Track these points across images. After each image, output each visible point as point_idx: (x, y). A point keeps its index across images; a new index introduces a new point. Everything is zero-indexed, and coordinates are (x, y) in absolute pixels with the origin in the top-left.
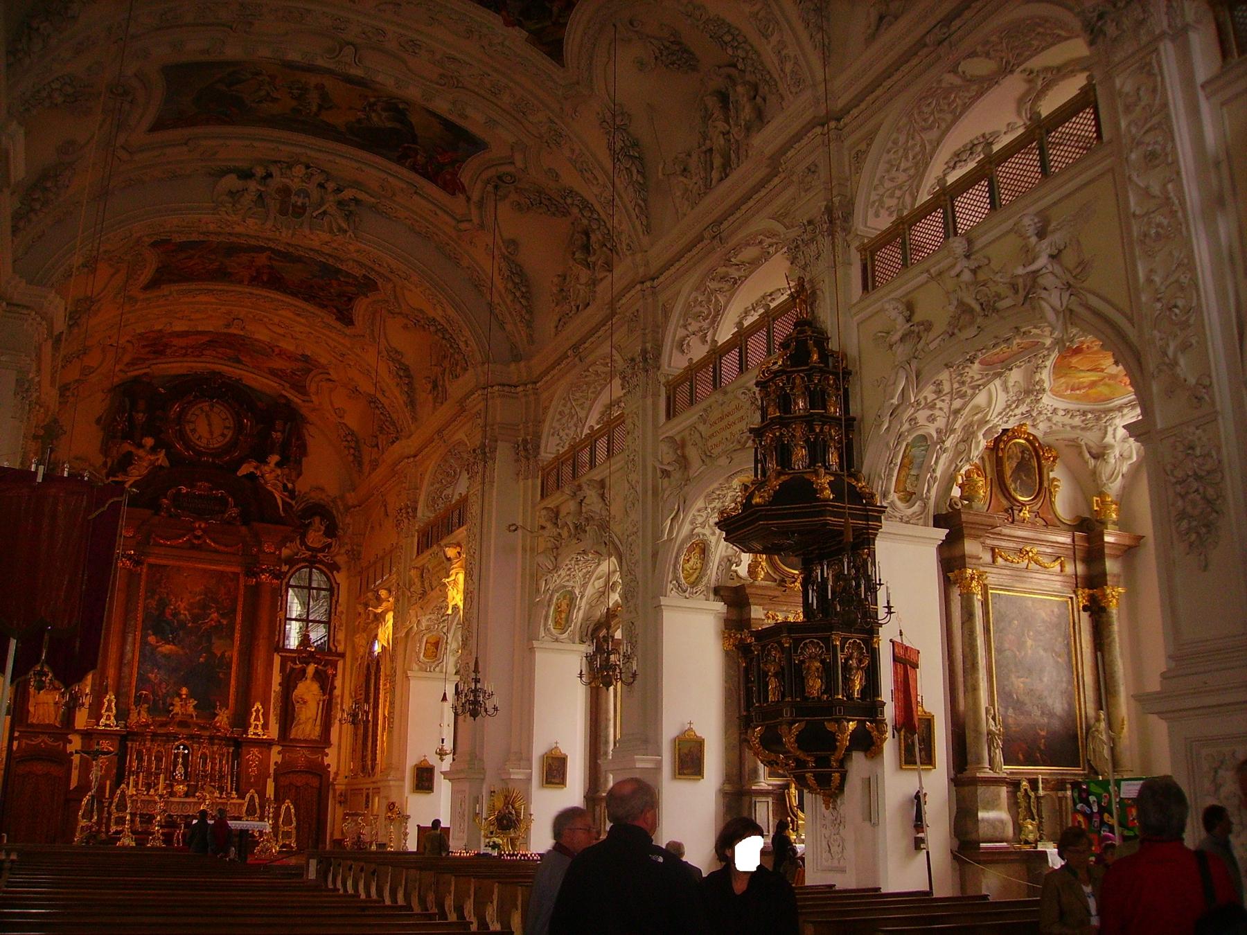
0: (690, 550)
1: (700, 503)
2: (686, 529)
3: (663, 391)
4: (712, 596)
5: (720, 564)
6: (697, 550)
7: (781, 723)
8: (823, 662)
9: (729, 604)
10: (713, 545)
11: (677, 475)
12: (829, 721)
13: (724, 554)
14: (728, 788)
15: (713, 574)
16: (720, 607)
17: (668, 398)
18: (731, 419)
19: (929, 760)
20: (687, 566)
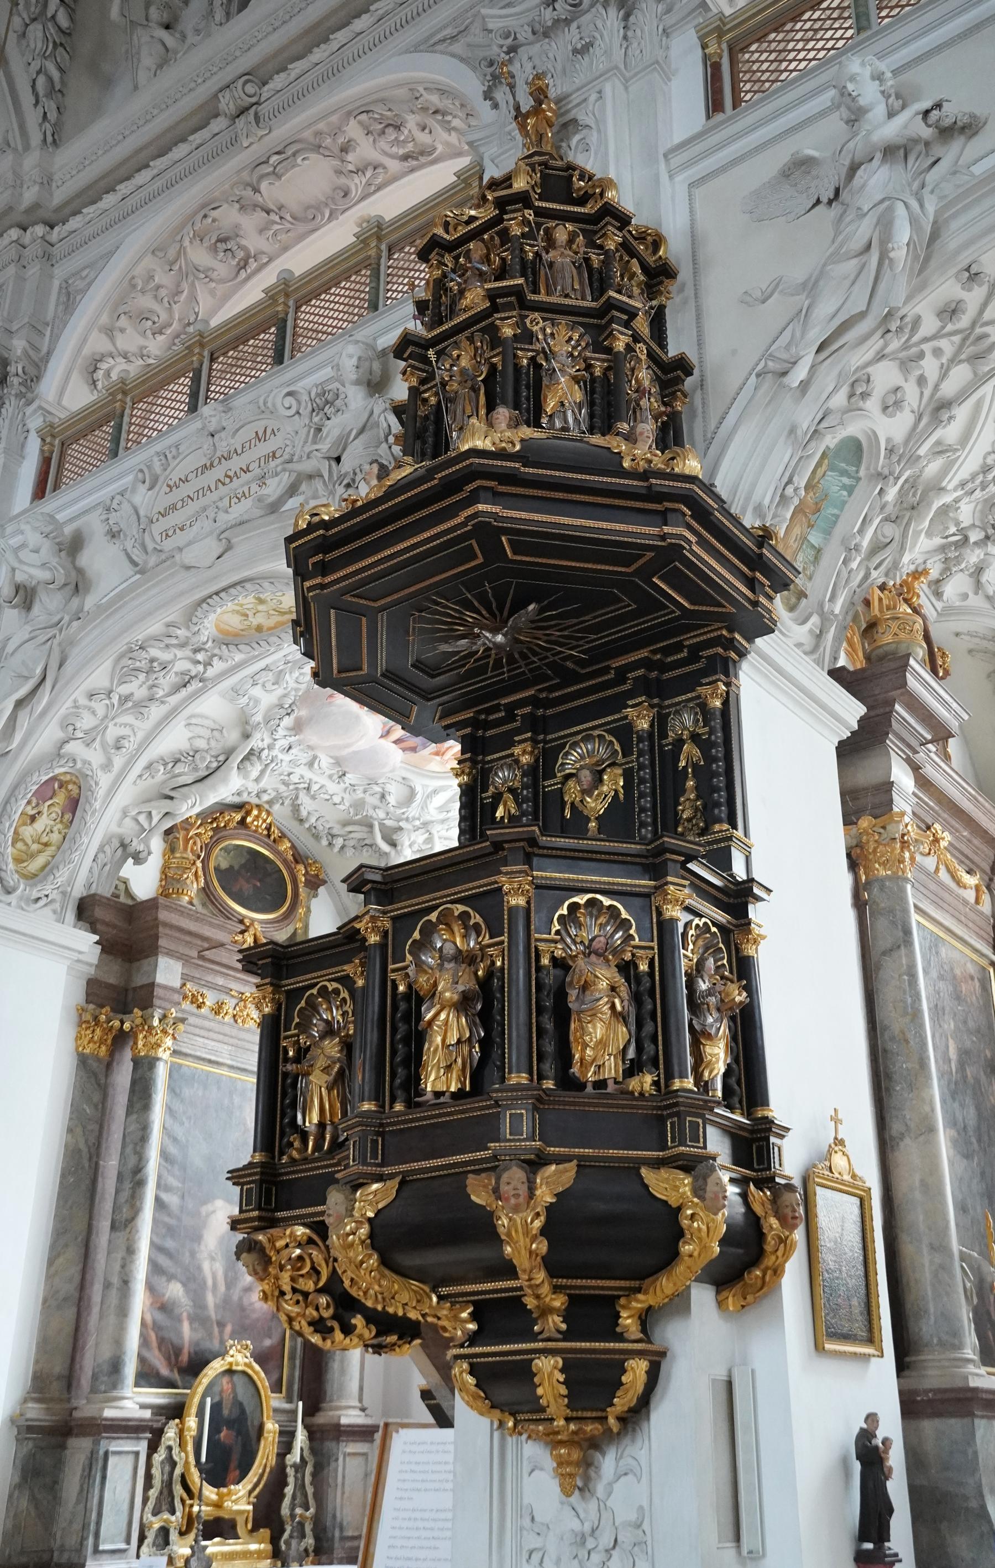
0: (45, 792)
1: (99, 676)
2: (49, 734)
3: (33, 448)
4: (71, 915)
5: (101, 849)
6: (60, 798)
7: (493, 1166)
8: (627, 969)
9: (108, 947)
10: (101, 792)
11: (49, 604)
12: (657, 1164)
13: (114, 829)
14: (35, 1412)
15: (80, 873)
16: (85, 943)
17: (46, 462)
18: (236, 463)
19: (871, 1338)
20: (28, 832)
